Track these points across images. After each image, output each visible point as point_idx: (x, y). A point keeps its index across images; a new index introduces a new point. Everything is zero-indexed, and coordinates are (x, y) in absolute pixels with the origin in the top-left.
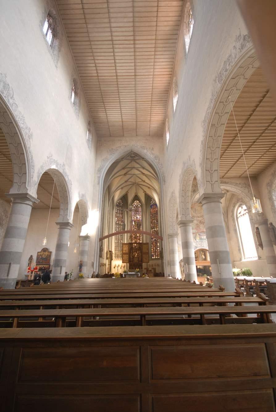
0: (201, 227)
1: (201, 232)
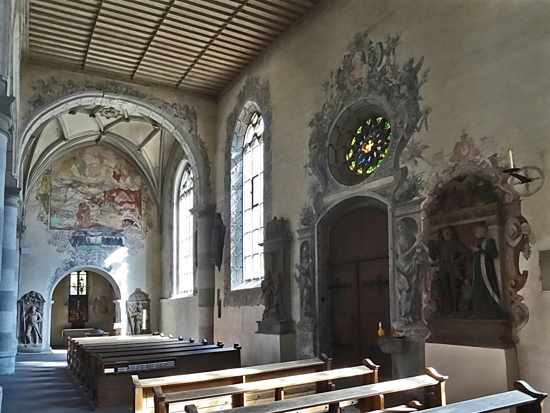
0: (92, 214)
1: (90, 227)
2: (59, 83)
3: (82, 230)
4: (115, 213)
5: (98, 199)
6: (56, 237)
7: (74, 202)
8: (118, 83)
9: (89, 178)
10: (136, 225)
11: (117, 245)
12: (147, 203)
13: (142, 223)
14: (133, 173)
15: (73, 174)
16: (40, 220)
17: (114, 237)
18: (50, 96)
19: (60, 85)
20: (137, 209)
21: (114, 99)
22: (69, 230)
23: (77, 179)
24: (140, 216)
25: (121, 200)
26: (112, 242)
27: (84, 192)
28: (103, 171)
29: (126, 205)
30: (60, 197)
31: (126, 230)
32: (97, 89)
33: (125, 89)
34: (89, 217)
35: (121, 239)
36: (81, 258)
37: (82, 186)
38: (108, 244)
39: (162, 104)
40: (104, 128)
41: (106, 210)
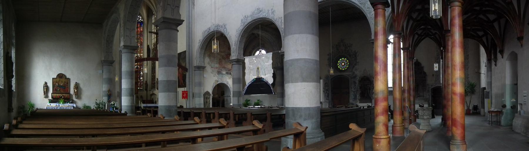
1: (222, 68)
35: (231, 73)
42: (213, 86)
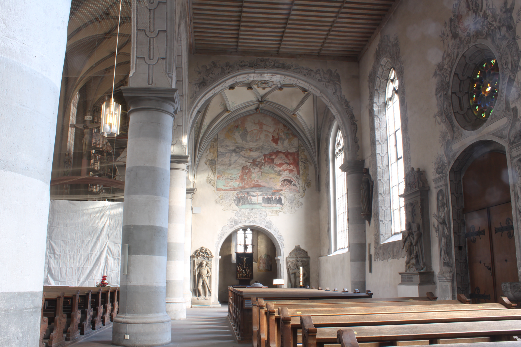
0: (253, 175)
1: (252, 188)
2: (219, 66)
3: (244, 190)
4: (275, 174)
5: (258, 162)
6: (222, 198)
7: (237, 165)
8: (266, 60)
9: (251, 143)
10: (294, 185)
11: (277, 204)
12: (304, 163)
13: (301, 183)
14: (291, 136)
15: (236, 140)
16: (208, 183)
17: (273, 197)
18: (212, 78)
19: (219, 67)
20: (295, 170)
21: (264, 73)
22: (233, 191)
23: (240, 145)
24: (298, 176)
25: (280, 162)
26: (272, 201)
27: (246, 156)
28: (263, 136)
29: (285, 167)
30: (226, 162)
31: (285, 189)
32: (250, 67)
33: (273, 64)
34: (251, 179)
35: (280, 199)
36: (244, 216)
37: (244, 151)
38: (268, 203)
39: (306, 71)
40: (262, 98)
41: (266, 171)
42: (223, 234)
